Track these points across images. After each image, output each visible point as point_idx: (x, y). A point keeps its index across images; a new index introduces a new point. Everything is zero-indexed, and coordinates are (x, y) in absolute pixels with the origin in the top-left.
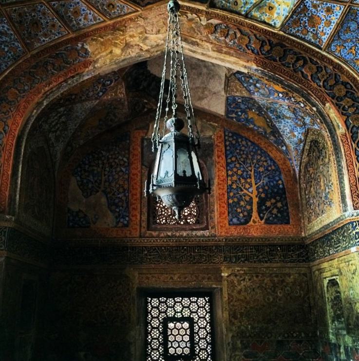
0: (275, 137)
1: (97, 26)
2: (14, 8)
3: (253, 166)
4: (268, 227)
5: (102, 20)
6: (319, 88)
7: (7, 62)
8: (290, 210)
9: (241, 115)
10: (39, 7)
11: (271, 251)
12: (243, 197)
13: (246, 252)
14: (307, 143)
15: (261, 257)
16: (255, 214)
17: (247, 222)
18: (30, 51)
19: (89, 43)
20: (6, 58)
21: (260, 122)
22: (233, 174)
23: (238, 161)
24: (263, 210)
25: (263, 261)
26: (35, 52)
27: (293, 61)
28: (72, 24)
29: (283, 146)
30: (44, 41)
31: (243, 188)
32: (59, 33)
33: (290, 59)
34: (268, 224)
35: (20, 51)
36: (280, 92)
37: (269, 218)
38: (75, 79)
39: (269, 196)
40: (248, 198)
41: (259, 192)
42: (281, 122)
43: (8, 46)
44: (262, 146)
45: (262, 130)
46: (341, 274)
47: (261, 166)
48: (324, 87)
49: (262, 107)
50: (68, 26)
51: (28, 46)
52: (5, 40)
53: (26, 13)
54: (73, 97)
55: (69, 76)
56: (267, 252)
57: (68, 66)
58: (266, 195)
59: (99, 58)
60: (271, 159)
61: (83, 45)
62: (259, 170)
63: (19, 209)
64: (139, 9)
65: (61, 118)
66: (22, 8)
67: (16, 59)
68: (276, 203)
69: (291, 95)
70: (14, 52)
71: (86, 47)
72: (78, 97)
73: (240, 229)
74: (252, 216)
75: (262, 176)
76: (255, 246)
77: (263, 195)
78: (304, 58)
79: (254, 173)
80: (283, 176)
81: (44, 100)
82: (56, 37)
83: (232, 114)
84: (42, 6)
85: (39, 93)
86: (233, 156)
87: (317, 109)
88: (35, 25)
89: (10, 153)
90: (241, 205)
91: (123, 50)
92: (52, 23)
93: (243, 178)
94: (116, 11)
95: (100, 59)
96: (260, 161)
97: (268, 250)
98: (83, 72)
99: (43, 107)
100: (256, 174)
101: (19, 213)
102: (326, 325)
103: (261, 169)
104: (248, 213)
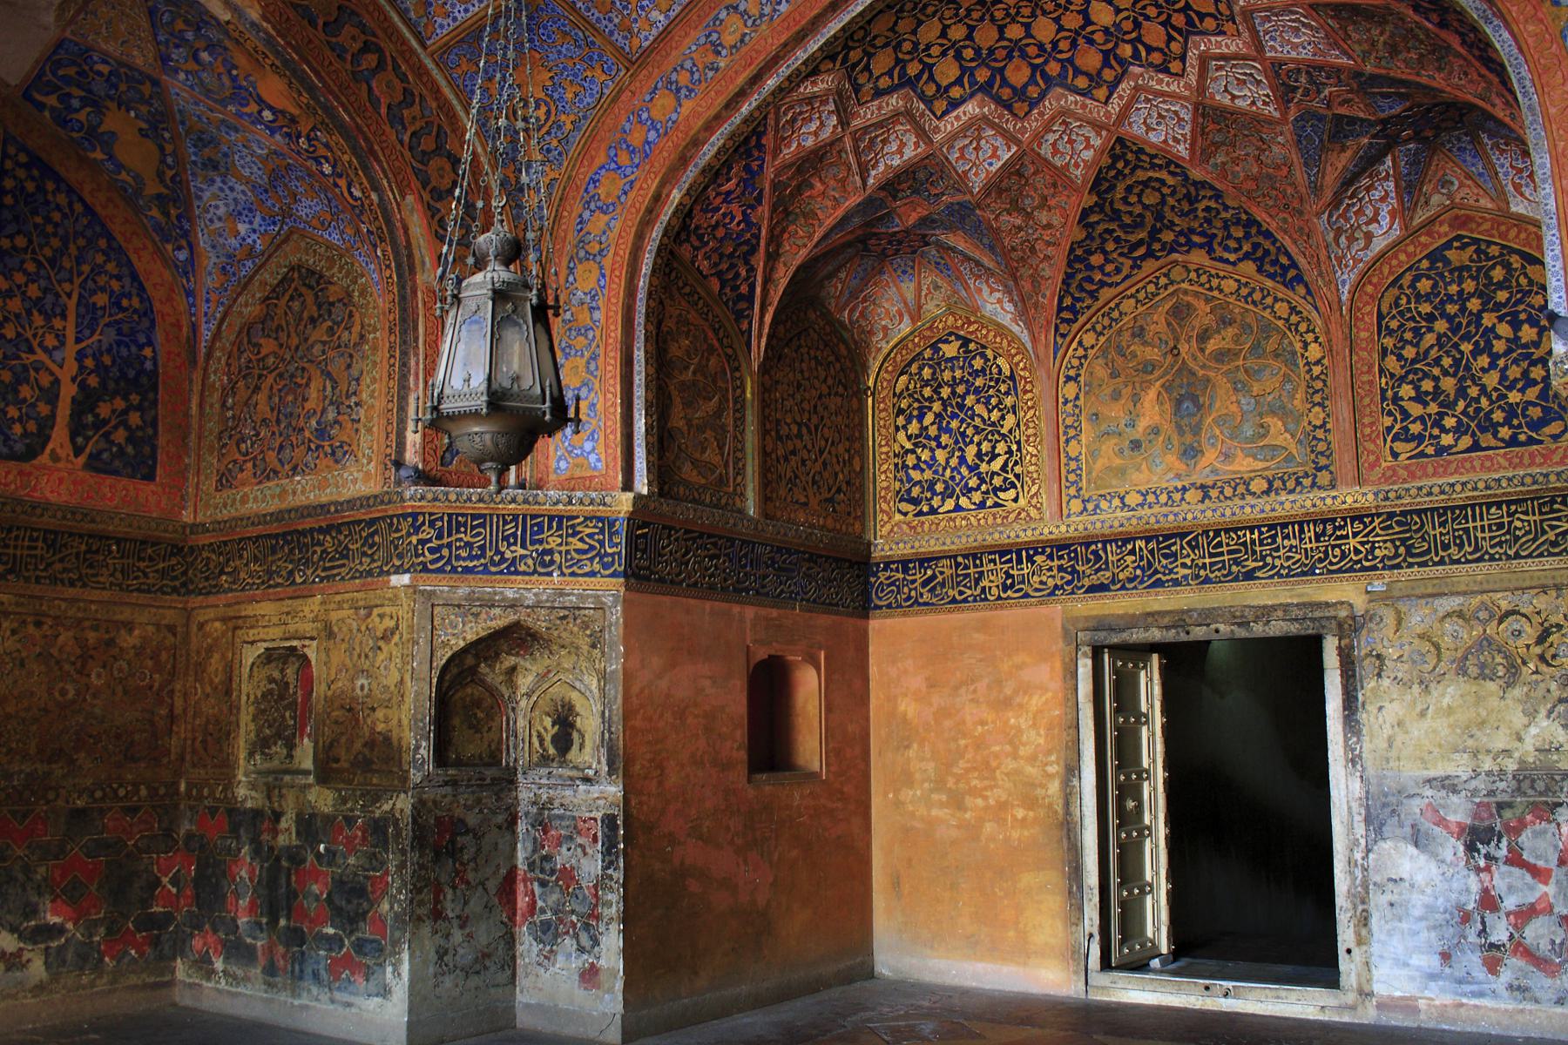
0: (167, 214)
3: (78, 281)
4: (92, 481)
6: (399, 147)
8: (162, 441)
9: (77, 111)
11: (88, 551)
12: (32, 373)
13: (16, 547)
14: (272, 265)
15: (58, 566)
16: (60, 436)
17: (31, 453)
21: (135, 154)
22: (11, 290)
23: (34, 252)
24: (85, 427)
25: (62, 581)
27: (357, 46)
29: (180, 248)
31: (35, 344)
33: (348, 37)
34: (98, 470)
36: (271, 108)
37: (100, 452)
39: (111, 385)
40: (45, 381)
41: (82, 368)
42: (213, 181)
44: (116, 228)
45: (129, 179)
46: (331, 635)
47: (103, 290)
48: (411, 149)
49: (178, 116)
56: (78, 555)
58: (103, 384)
60: (134, 276)
62: (94, 299)
68: (125, 412)
69: (304, 127)
73: (8, 473)
74: (48, 438)
75: (102, 322)
76: (46, 531)
77: (93, 381)
78: (380, 50)
79: (78, 304)
80: (159, 337)
83: (47, 94)
86: (19, 232)
87: (381, 199)
90: (21, 396)
93: (40, 311)
96: (99, 273)
97: (83, 547)
100: (82, 310)
102: (226, 767)
103: (101, 299)
104: (39, 425)
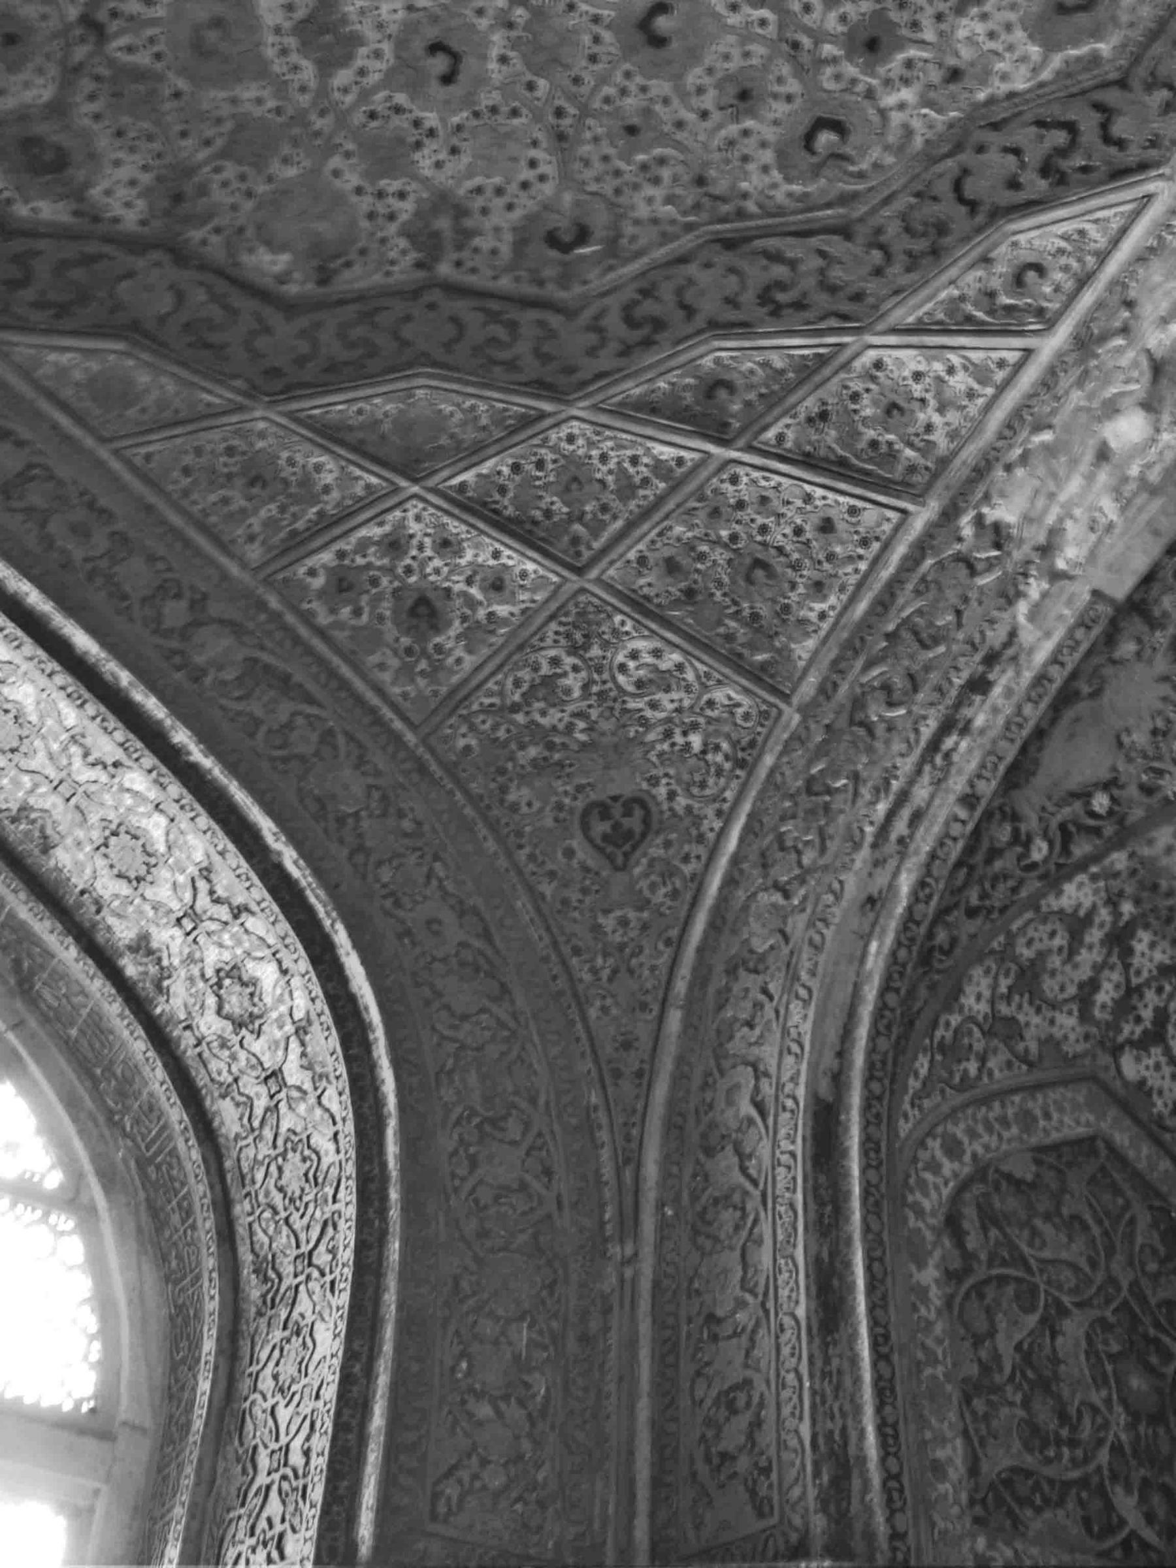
1: (1011, 399)
2: (632, 555)
5: (1012, 357)
7: (718, 798)
10: (728, 488)
18: (786, 698)
19: (1003, 495)
20: (711, 781)
26: (809, 687)
28: (900, 468)
30: (822, 616)
32: (865, 543)
35: (747, 716)
38: (997, 691)
43: (694, 726)
50: (884, 486)
51: (768, 679)
52: (671, 707)
53: (690, 547)
54: (1101, 802)
55: (954, 693)
57: (942, 649)
59: (1061, 520)
61: (979, 520)
63: (892, 1512)
64: (1150, 187)
65: (1130, 951)
66: (660, 534)
67: (744, 763)
70: (728, 737)
71: (992, 514)
72: (1133, 791)
81: (896, 874)
82: (863, 566)
84: (734, 480)
85: (857, 846)
88: (759, 574)
89: (792, 1206)
91: (1149, 406)
92: (815, 519)
94: (1058, 276)
95: (1069, 524)
98: (1013, 634)
99: (900, 910)
101: (896, 1536)
